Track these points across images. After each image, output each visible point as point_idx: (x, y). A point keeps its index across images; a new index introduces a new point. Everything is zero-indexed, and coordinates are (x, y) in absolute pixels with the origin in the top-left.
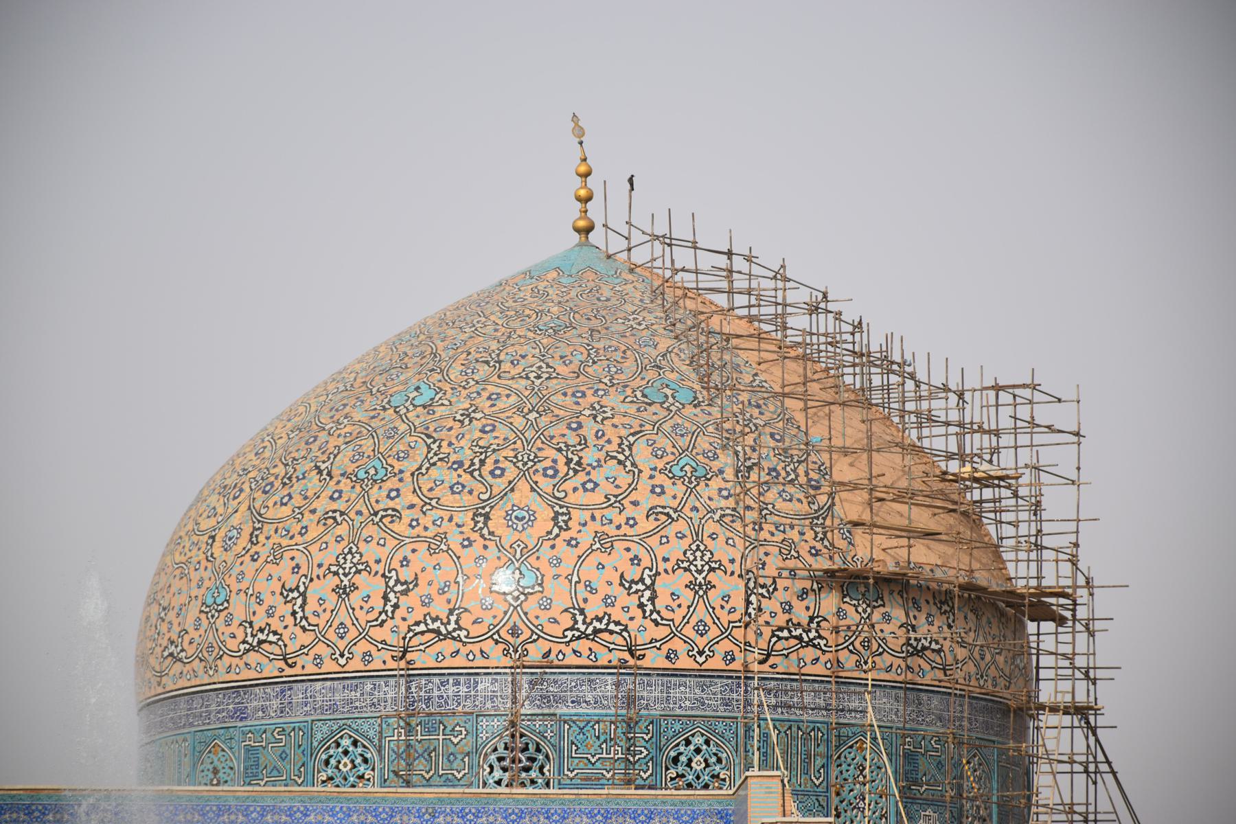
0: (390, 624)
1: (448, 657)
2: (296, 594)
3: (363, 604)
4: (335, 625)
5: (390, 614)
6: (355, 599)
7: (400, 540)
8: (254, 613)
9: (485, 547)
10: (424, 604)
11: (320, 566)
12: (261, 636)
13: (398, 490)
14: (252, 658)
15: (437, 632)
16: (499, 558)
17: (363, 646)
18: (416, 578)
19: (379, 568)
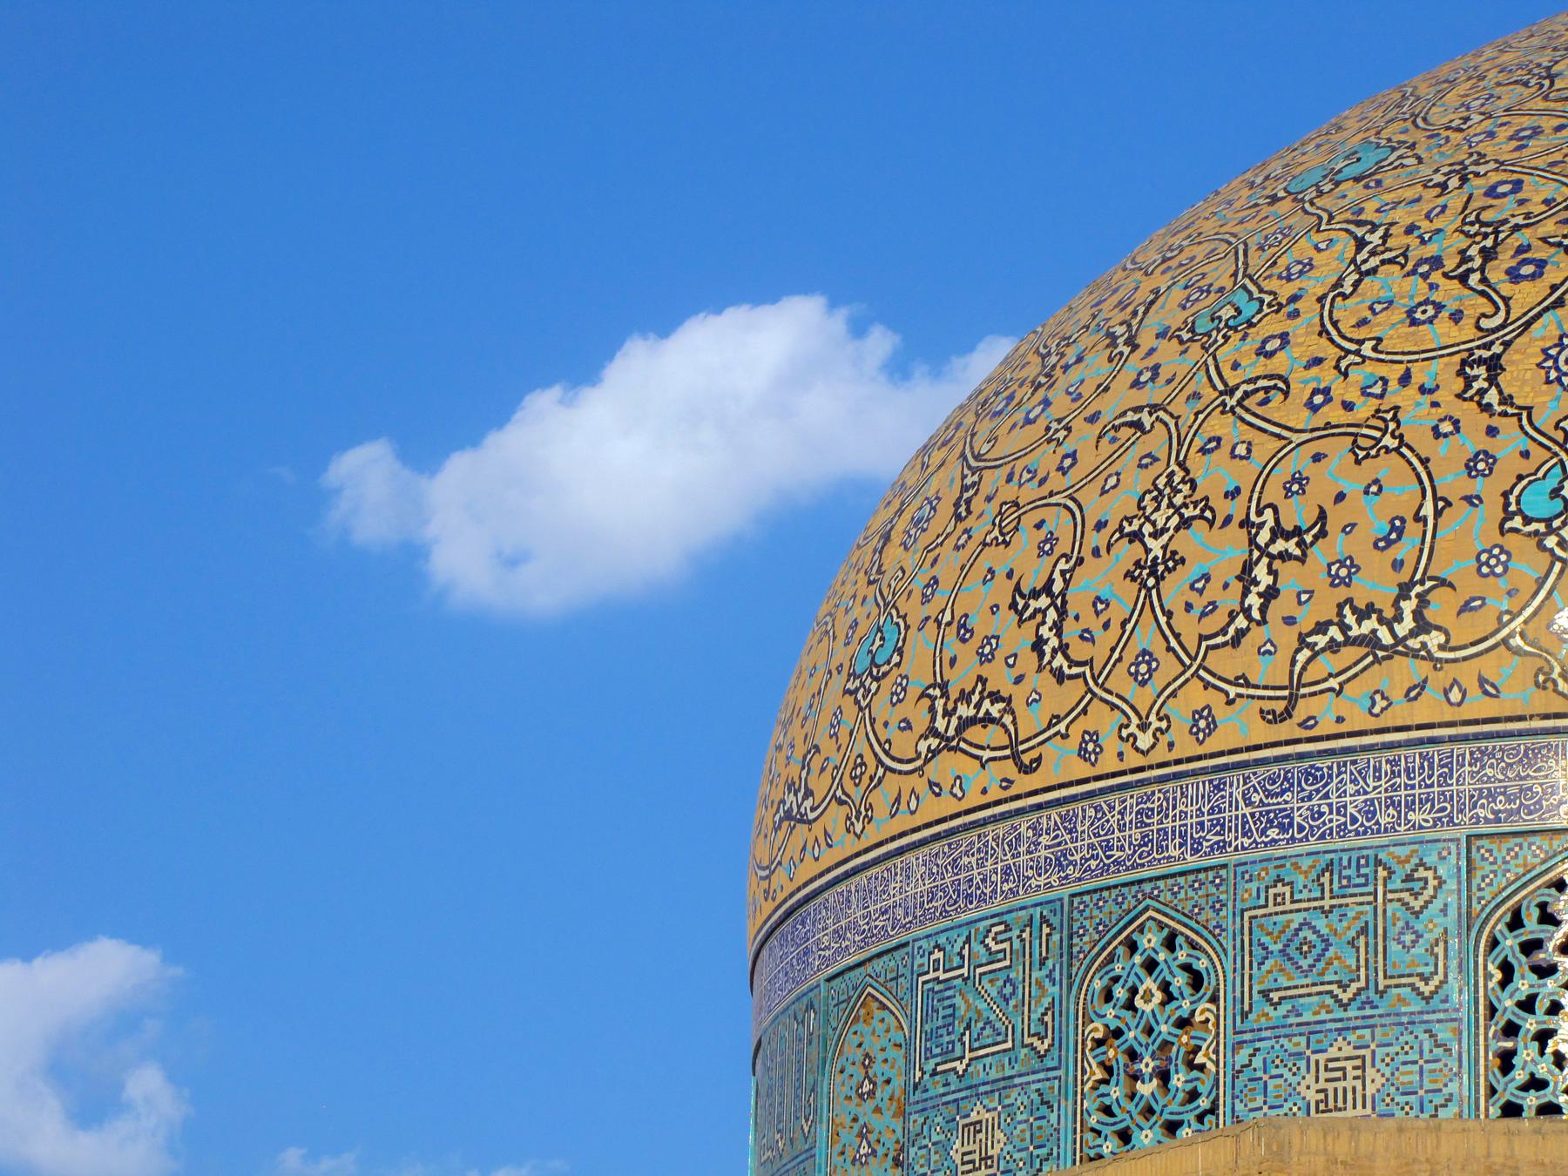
0: (1257, 635)
1: (1397, 695)
2: (1044, 601)
3: (1193, 597)
4: (1129, 657)
5: (1256, 615)
6: (1174, 589)
7: (1281, 432)
8: (953, 662)
9: (1492, 431)
10: (1335, 581)
11: (1100, 526)
12: (965, 711)
13: (1284, 337)
14: (947, 766)
15: (1371, 641)
16: (1525, 455)
17: (1195, 696)
18: (1322, 516)
19: (1236, 509)
